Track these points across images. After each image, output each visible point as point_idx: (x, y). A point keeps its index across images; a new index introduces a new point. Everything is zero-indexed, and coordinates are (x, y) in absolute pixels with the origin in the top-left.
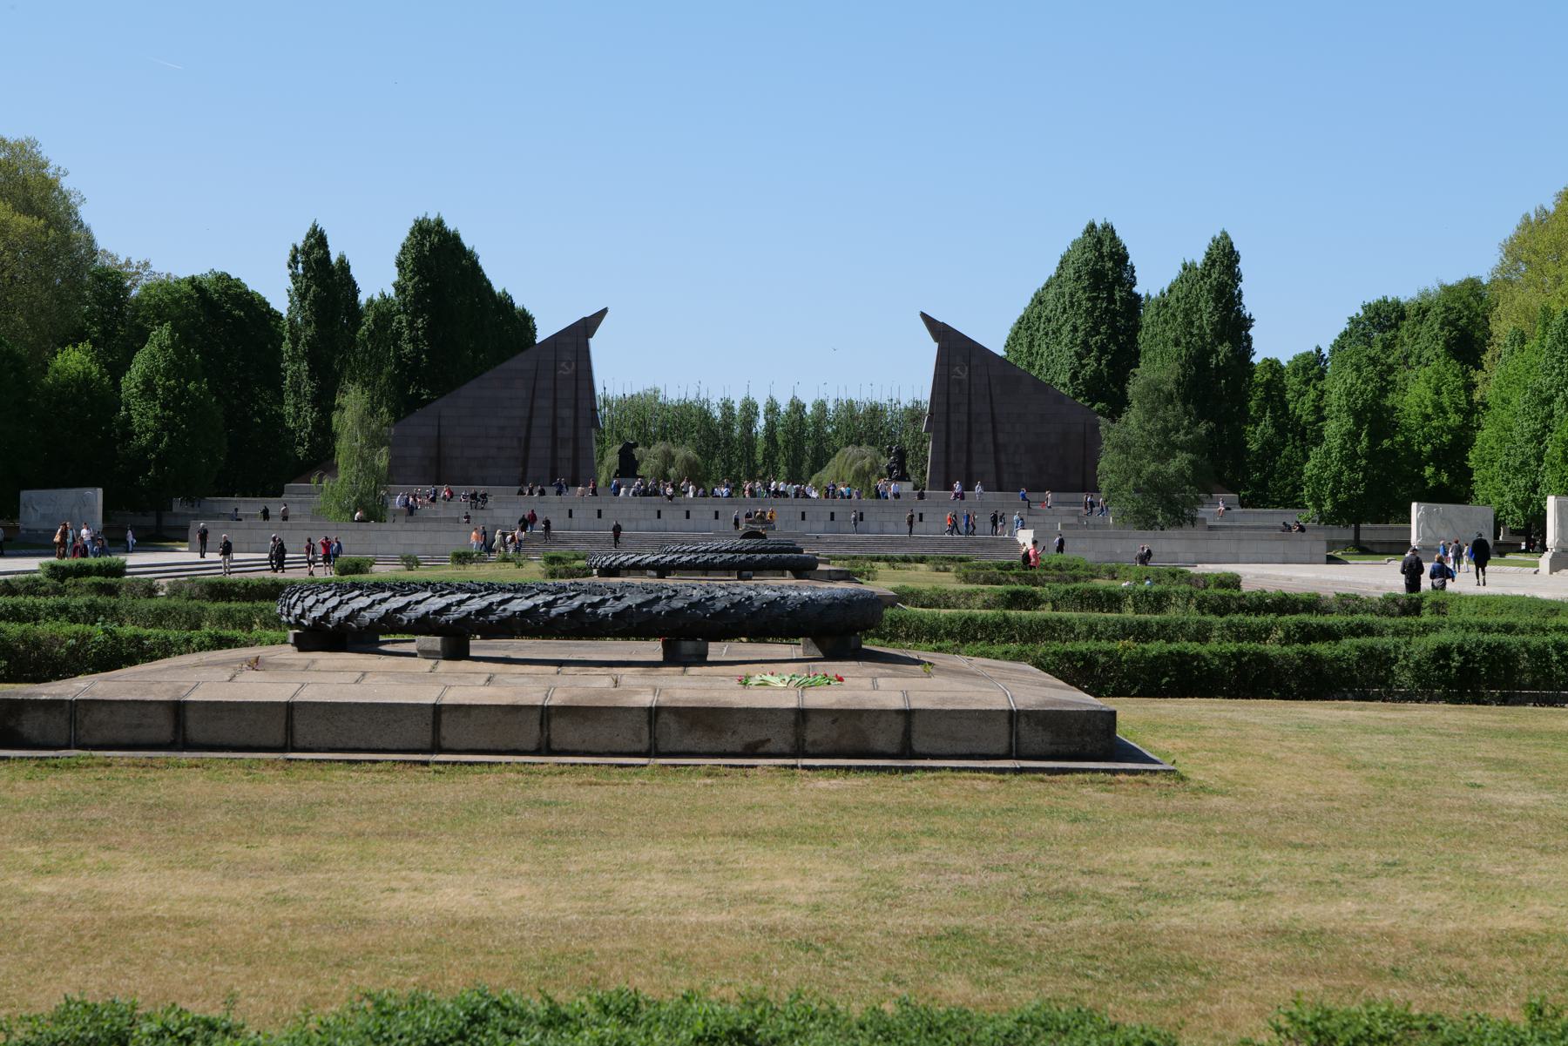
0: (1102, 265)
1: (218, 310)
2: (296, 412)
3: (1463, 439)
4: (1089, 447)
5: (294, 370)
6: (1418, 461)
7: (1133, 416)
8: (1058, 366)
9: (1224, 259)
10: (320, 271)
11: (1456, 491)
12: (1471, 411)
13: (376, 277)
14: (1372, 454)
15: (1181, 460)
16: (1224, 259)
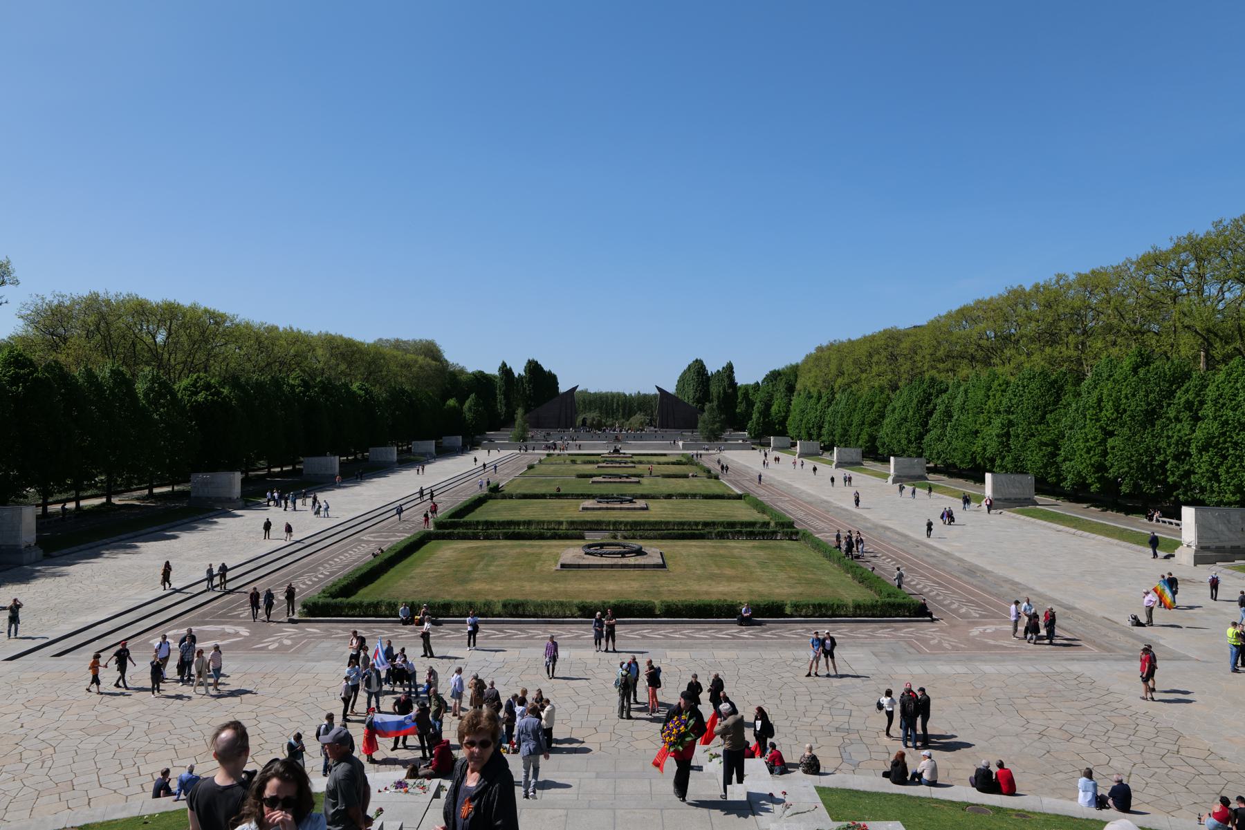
0: (698, 368)
1: (481, 380)
2: (501, 408)
3: (785, 418)
4: (697, 420)
5: (500, 397)
6: (774, 424)
7: (706, 415)
8: (689, 397)
9: (730, 368)
10: (506, 371)
11: (783, 433)
12: (788, 412)
13: (519, 370)
14: (764, 422)
15: (718, 425)
16: (730, 368)
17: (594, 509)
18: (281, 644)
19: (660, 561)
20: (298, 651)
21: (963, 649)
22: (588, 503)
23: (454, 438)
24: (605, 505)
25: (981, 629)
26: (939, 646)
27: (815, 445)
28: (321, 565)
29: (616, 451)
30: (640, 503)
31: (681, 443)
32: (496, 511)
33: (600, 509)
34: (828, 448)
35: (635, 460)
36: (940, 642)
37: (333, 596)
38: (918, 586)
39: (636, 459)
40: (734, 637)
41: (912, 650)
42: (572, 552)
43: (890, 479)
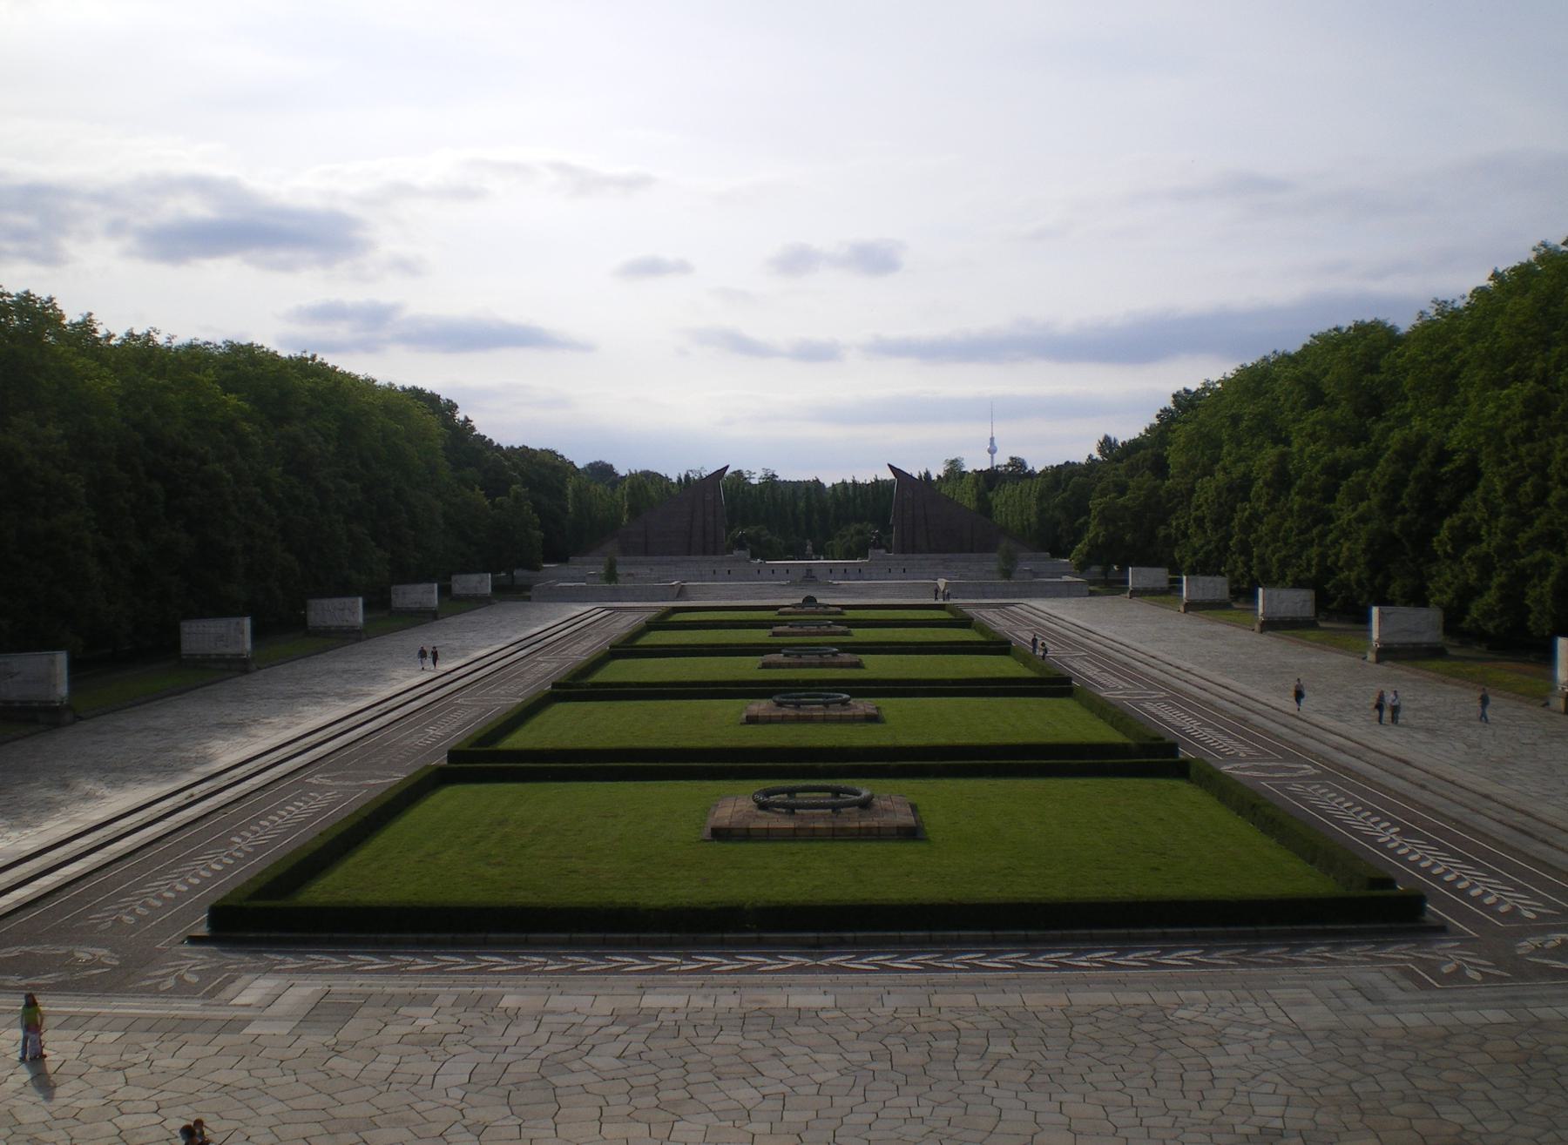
17: (769, 720)
18: (180, 978)
19: (910, 820)
20: (211, 994)
21: (1501, 979)
22: (760, 706)
23: (474, 579)
24: (789, 711)
25: (1534, 941)
26: (1458, 976)
27: (1216, 587)
28: (237, 833)
29: (810, 600)
30: (863, 706)
31: (942, 583)
32: (567, 727)
33: (783, 720)
34: (1243, 594)
35: (844, 619)
36: (1460, 970)
37: (257, 895)
38: (1420, 861)
39: (850, 614)
40: (1063, 967)
41: (1406, 984)
42: (734, 803)
43: (1371, 656)
